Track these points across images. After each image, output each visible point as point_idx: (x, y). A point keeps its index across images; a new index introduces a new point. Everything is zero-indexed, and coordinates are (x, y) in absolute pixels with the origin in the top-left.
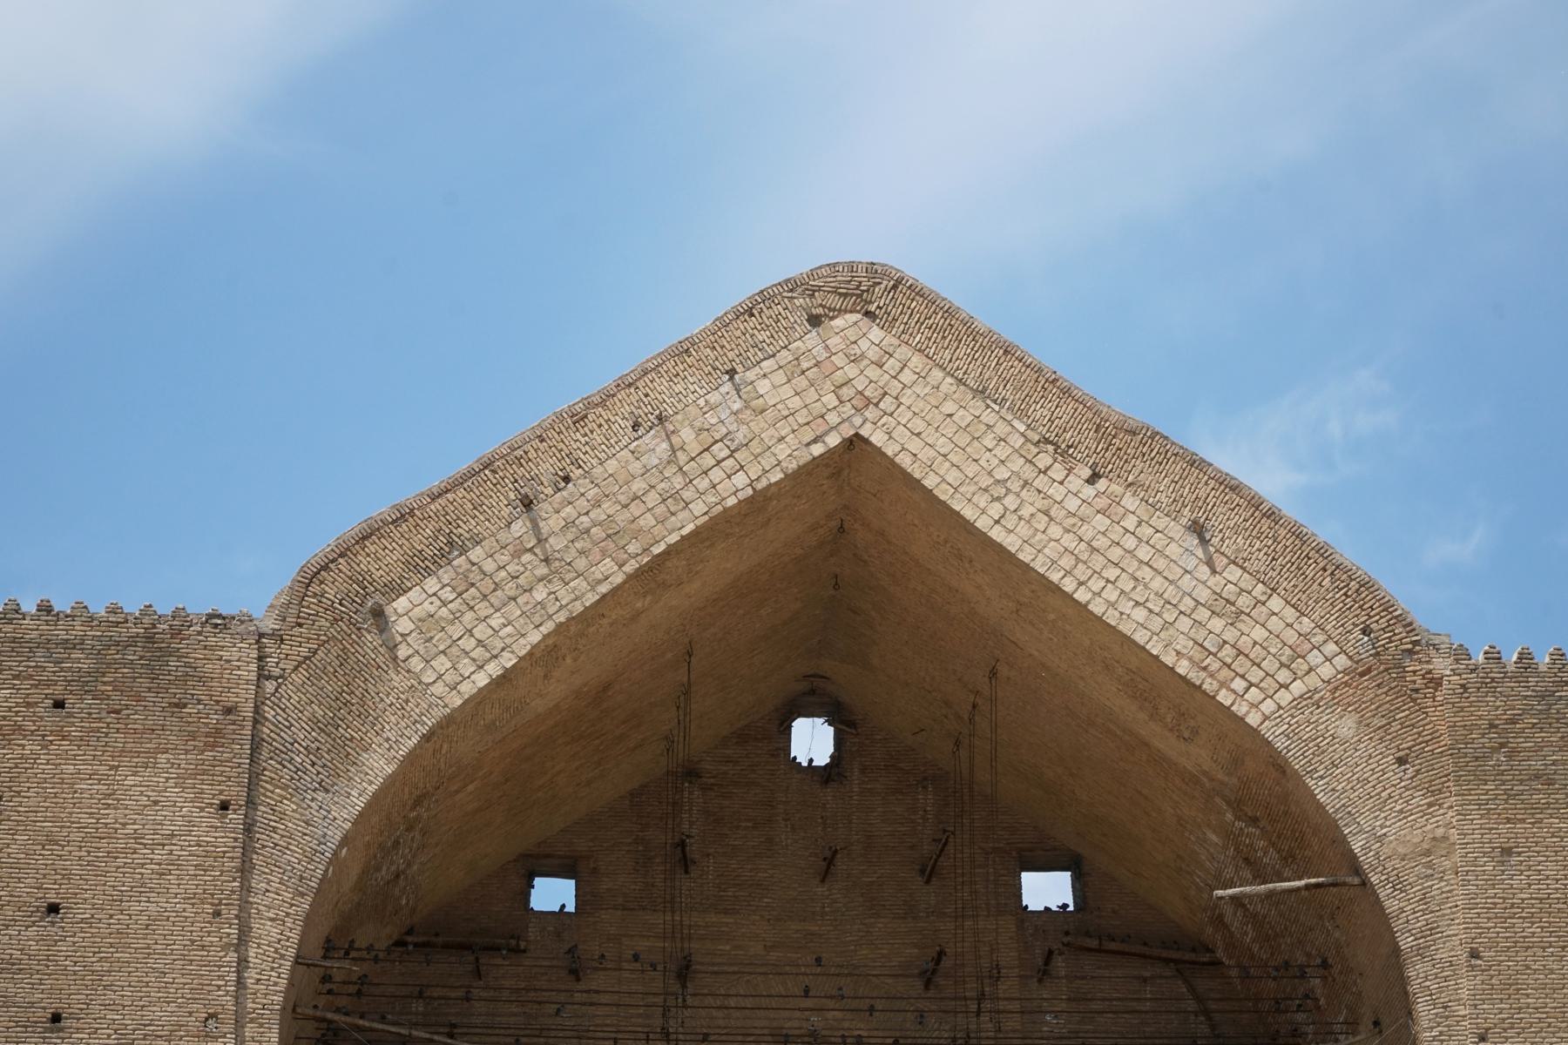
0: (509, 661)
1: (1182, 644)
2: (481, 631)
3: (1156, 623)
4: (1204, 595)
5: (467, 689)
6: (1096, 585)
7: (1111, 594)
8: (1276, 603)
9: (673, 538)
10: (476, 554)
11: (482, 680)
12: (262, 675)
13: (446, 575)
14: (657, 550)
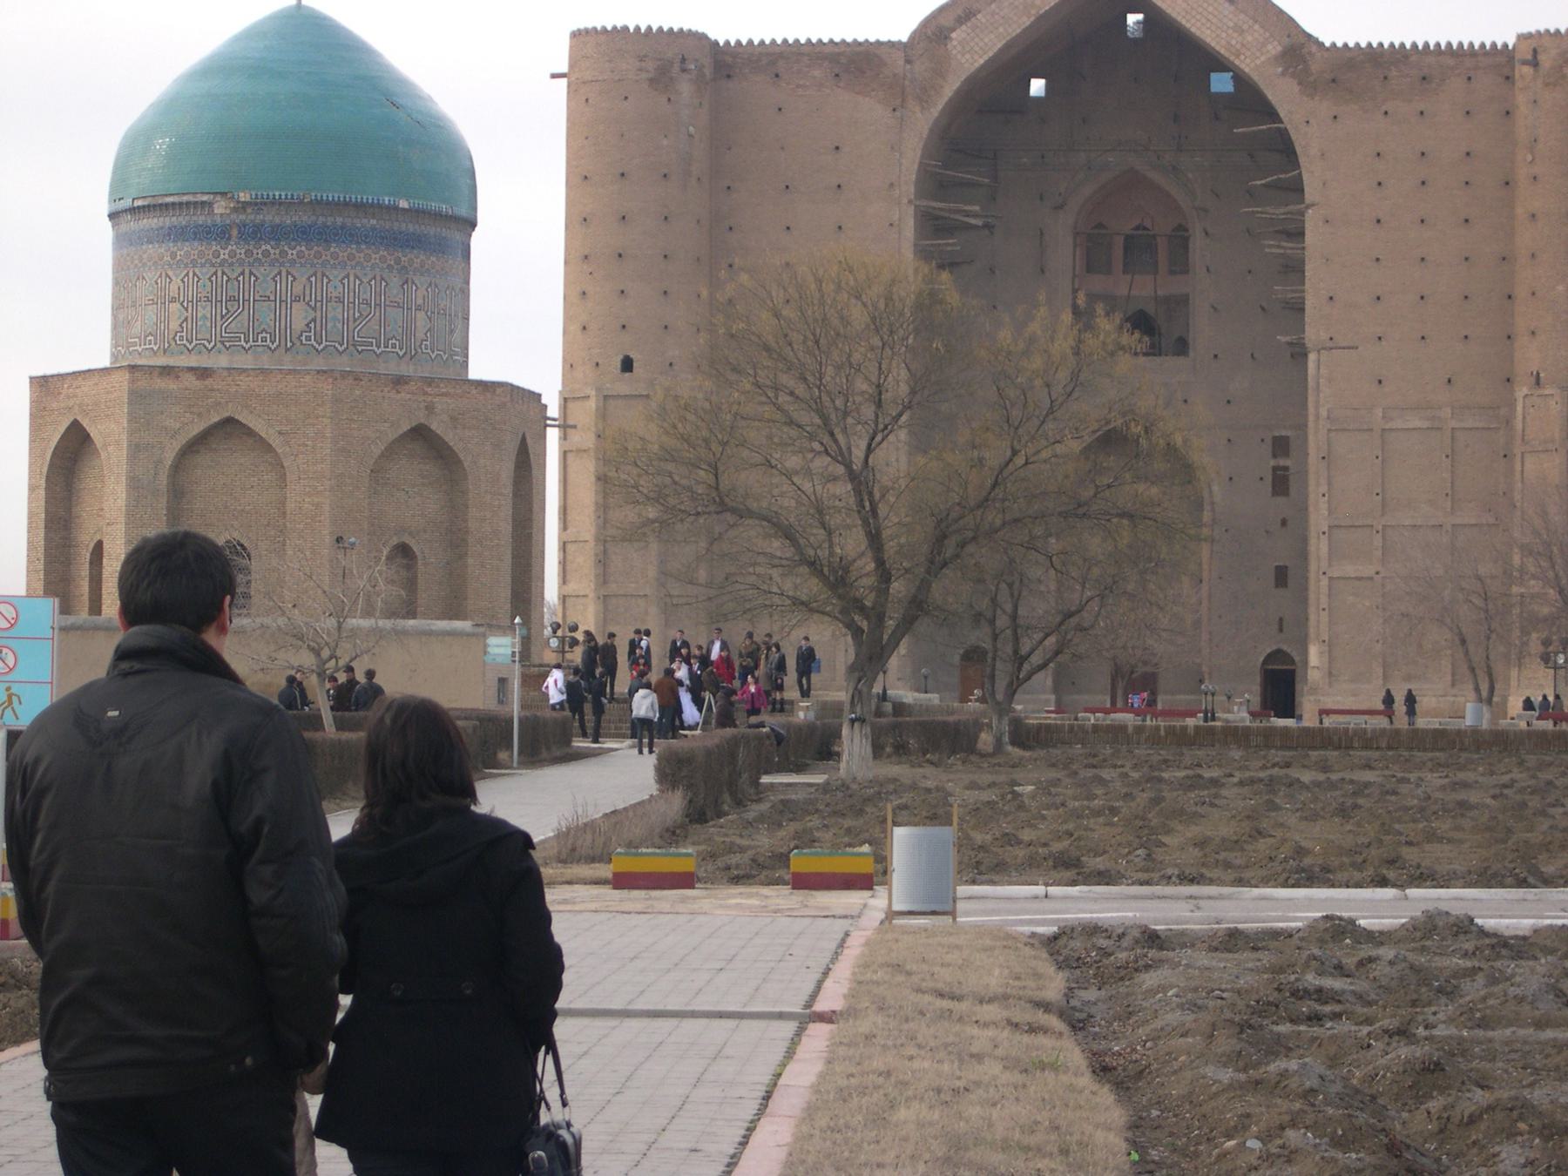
0: (991, 54)
1: (1223, 42)
2: (981, 44)
3: (1214, 35)
4: (1231, 24)
5: (977, 65)
6: (1193, 21)
7: (1199, 24)
8: (1257, 27)
9: (1047, 8)
10: (979, 16)
11: (982, 61)
12: (908, 61)
13: (969, 24)
14: (1042, 12)
